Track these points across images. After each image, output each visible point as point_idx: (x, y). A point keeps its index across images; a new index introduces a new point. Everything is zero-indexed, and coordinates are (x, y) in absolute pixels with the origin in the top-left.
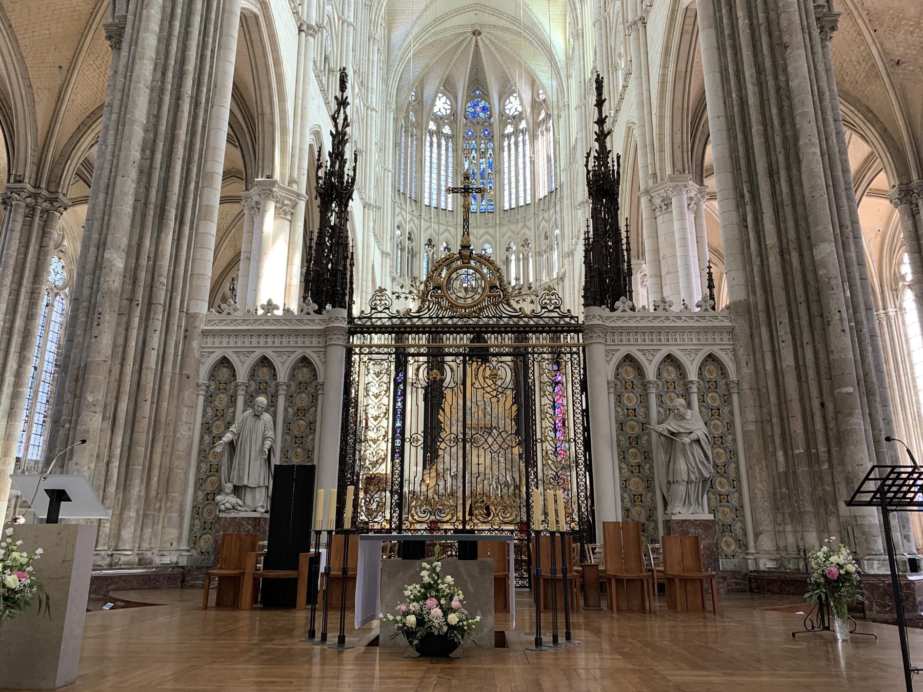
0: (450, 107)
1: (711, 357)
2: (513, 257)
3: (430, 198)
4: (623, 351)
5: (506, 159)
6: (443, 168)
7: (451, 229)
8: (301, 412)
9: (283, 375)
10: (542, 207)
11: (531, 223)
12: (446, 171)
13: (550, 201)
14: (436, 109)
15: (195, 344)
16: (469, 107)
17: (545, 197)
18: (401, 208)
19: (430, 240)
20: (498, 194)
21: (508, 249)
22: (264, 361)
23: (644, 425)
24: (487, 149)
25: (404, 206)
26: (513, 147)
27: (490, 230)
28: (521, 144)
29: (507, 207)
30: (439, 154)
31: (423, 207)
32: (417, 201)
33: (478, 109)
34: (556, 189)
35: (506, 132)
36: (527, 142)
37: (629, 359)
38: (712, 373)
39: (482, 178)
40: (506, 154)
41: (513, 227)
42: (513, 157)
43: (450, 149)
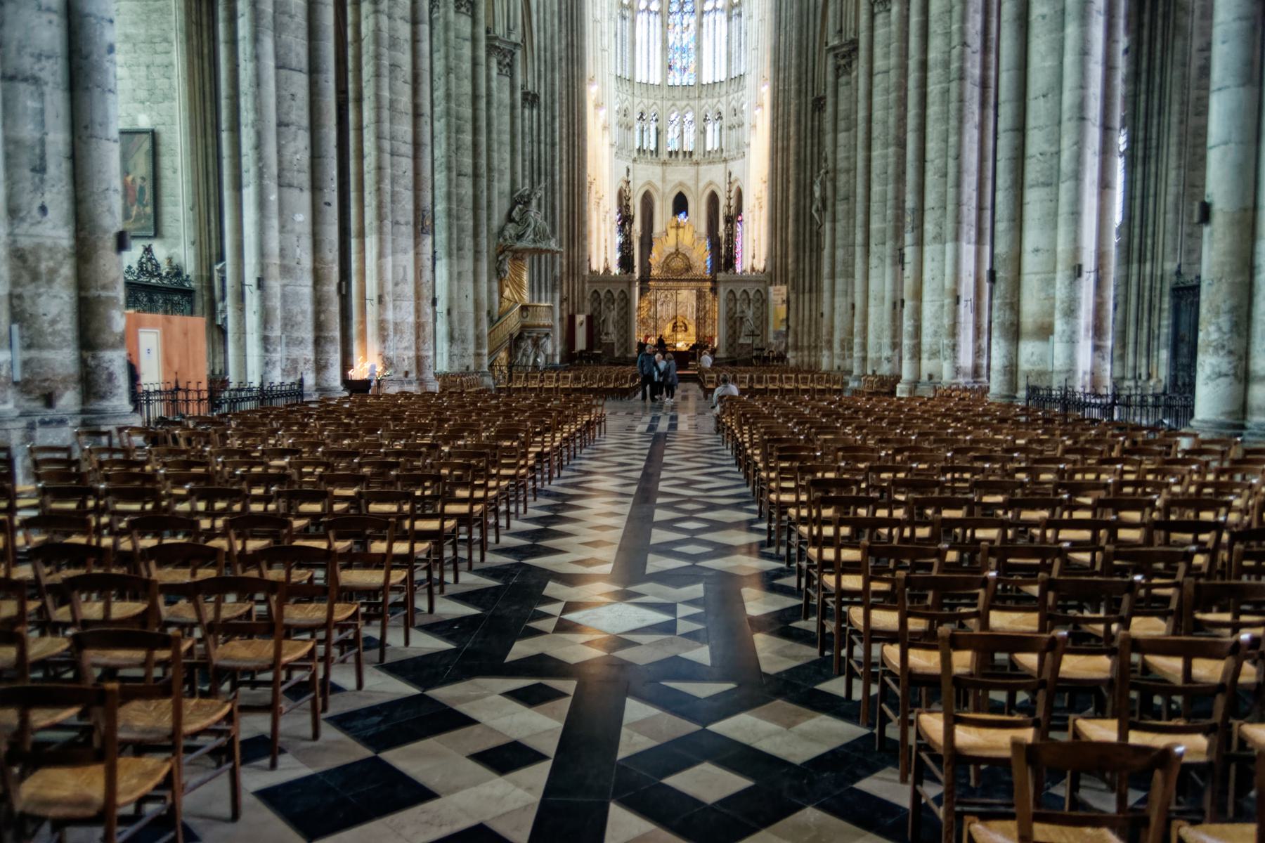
1: (758, 290)
2: (709, 128)
4: (729, 289)
7: (659, 102)
8: (622, 309)
9: (616, 295)
11: (724, 100)
15: (587, 286)
19: (642, 114)
21: (705, 120)
22: (609, 291)
23: (735, 313)
27: (692, 103)
29: (704, 83)
32: (631, 81)
37: (731, 291)
38: (758, 296)
41: (710, 101)
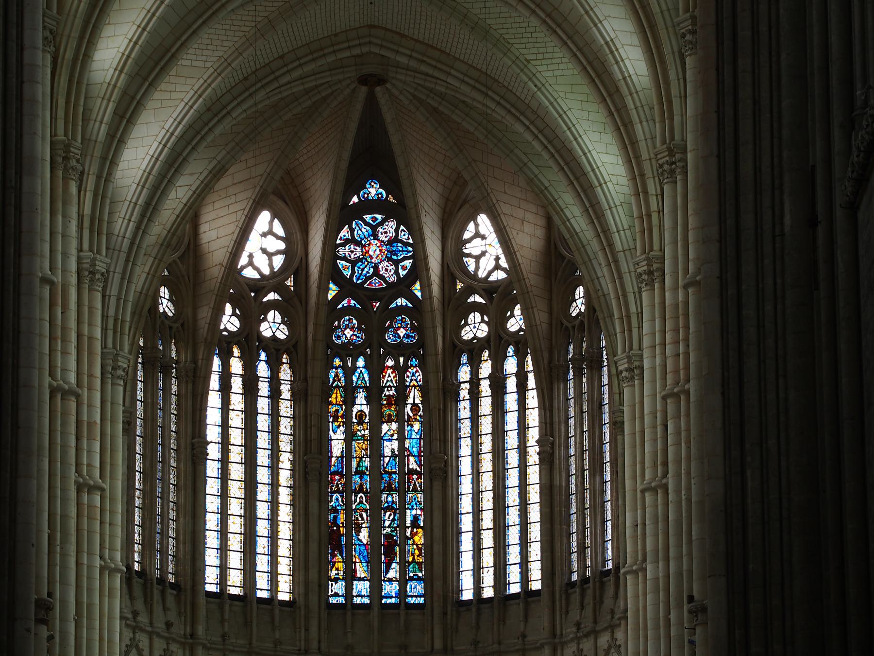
0: (282, 246)
3: (224, 568)
5: (465, 428)
6: (263, 458)
10: (575, 614)
12: (274, 469)
13: (599, 602)
14: (243, 260)
16: (346, 242)
17: (584, 580)
18: (135, 628)
20: (437, 548)
24: (402, 390)
25: (143, 619)
26: (485, 388)
28: (511, 384)
30: (250, 413)
31: (202, 600)
33: (374, 249)
34: (617, 568)
35: (467, 334)
36: (532, 382)
39: (390, 489)
40: (465, 411)
42: (486, 425)
43: (286, 391)
